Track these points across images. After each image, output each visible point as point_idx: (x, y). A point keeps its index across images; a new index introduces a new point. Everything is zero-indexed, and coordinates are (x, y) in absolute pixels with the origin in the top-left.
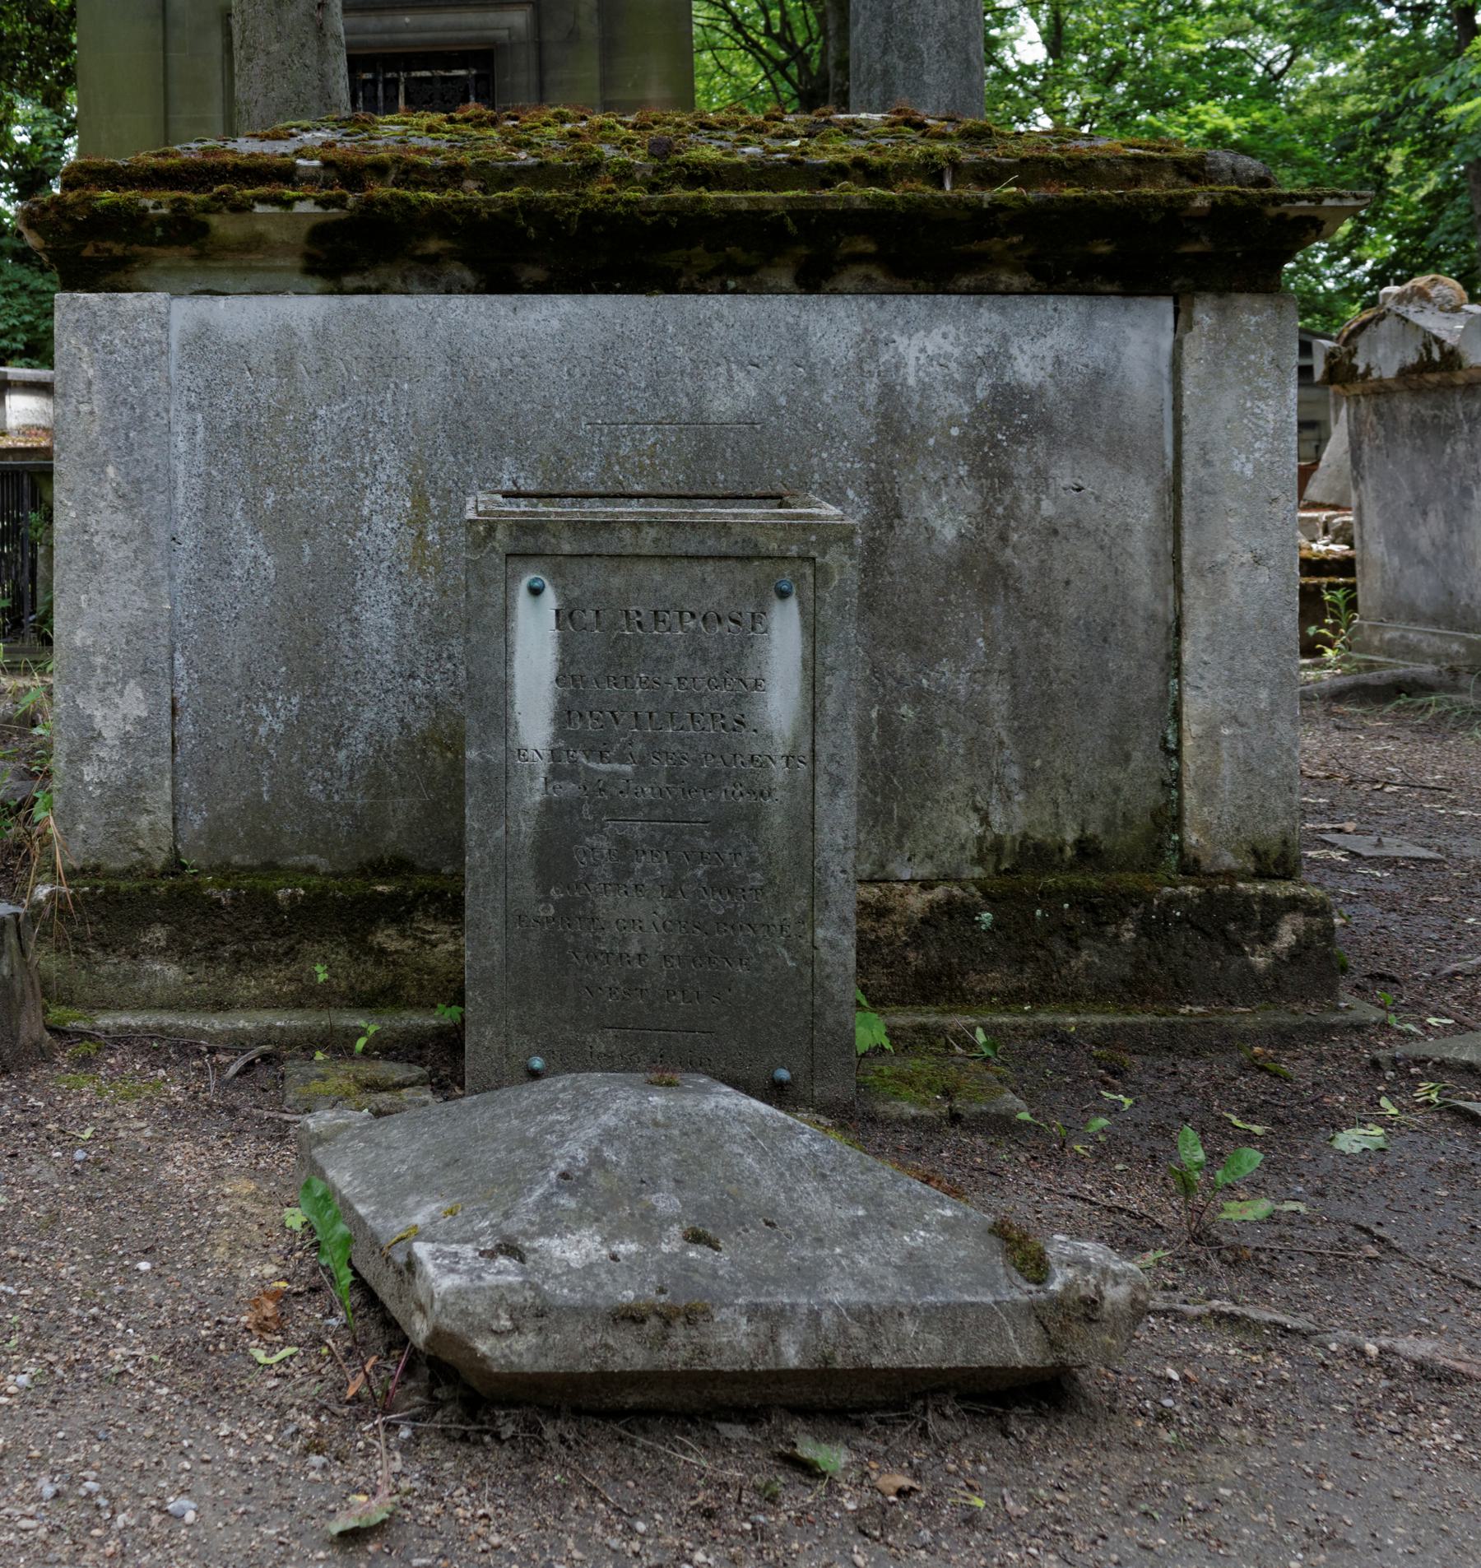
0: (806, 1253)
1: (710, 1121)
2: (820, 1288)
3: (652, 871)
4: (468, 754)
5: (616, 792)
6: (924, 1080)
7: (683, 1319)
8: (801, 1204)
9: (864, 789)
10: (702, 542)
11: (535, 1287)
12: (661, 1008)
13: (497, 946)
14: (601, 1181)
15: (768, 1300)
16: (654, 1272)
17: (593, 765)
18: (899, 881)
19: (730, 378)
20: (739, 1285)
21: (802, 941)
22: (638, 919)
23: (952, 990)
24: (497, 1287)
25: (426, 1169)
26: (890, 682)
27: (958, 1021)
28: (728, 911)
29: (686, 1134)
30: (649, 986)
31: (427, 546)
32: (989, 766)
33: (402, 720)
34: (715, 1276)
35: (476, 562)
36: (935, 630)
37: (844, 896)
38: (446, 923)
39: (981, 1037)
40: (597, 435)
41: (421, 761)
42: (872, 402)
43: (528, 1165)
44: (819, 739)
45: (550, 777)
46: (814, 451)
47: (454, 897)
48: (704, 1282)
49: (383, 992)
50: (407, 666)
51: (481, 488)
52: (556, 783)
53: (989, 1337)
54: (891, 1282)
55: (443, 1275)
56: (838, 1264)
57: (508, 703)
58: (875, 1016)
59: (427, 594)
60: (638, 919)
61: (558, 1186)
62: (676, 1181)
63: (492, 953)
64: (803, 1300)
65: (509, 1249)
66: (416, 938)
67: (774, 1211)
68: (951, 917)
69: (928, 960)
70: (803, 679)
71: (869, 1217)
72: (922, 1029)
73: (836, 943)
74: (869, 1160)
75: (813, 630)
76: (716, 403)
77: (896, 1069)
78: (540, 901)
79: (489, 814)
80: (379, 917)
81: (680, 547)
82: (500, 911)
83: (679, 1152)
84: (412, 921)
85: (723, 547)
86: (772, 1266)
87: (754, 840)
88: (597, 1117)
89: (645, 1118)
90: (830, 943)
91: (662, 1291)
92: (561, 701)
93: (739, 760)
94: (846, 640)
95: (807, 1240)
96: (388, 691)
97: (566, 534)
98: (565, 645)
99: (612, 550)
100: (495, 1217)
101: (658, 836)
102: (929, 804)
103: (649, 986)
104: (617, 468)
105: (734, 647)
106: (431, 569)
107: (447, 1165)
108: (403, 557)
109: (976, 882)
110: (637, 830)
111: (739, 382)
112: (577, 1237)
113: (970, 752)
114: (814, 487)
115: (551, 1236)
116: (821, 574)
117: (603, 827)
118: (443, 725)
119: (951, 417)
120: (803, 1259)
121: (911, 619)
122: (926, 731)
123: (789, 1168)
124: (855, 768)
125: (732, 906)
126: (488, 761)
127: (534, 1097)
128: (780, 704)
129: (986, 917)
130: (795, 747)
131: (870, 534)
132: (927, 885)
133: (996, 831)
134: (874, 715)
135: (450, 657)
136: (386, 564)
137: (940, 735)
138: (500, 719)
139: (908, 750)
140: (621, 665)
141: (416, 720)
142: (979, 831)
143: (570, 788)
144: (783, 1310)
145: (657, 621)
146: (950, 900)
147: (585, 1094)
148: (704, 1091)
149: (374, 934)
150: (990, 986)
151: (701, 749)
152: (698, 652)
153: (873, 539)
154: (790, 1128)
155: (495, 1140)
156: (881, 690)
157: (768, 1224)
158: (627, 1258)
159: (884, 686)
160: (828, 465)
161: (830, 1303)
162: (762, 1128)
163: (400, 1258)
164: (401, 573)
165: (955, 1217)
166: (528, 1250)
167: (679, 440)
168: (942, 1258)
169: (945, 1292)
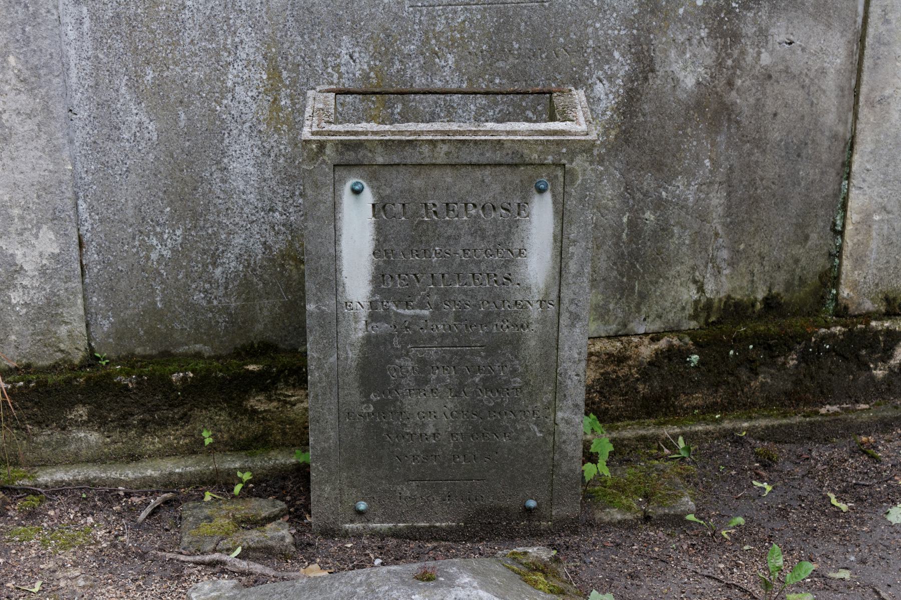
3: (444, 380)
4: (308, 307)
5: (418, 328)
10: (482, 154)
12: (449, 466)
13: (332, 434)
17: (400, 311)
21: (547, 420)
28: (497, 403)
30: (441, 453)
45: (369, 321)
52: (374, 324)
57: (337, 271)
60: (433, 412)
63: (329, 438)
70: (554, 248)
75: (562, 214)
78: (363, 403)
79: (324, 347)
82: (334, 411)
85: (498, 157)
87: (516, 357)
90: (566, 421)
93: (507, 304)
97: (380, 149)
99: (414, 161)
101: (448, 357)
103: (441, 453)
105: (504, 228)
110: (432, 353)
116: (570, 176)
125: (499, 400)
126: (323, 311)
128: (537, 265)
130: (547, 294)
145: (448, 210)
151: (479, 298)
152: (478, 232)
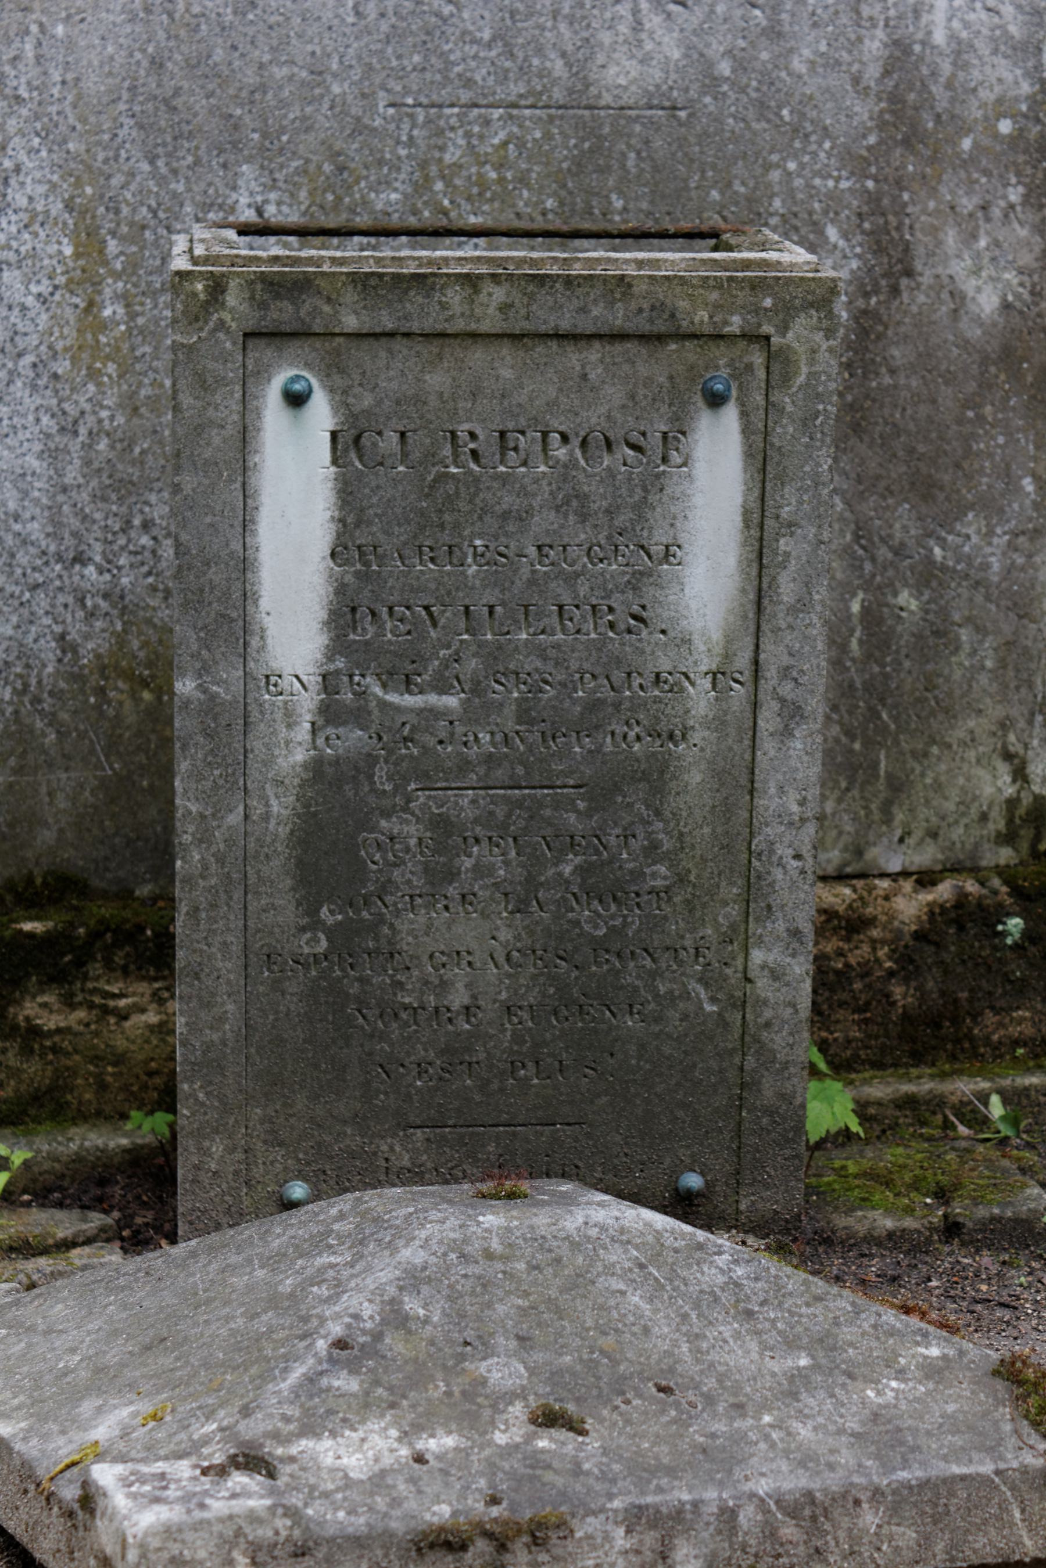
0: (720, 1427)
1: (576, 1246)
2: (738, 1473)
3: (491, 870)
4: (178, 686)
5: (431, 741)
6: (908, 1177)
7: (526, 1539)
8: (713, 1356)
9: (835, 730)
10: (583, 310)
11: (292, 1513)
12: (502, 1090)
13: (230, 1007)
14: (400, 1347)
15: (658, 1499)
16: (482, 1474)
17: (393, 698)
18: (883, 875)
19: (638, 26)
20: (614, 1481)
21: (729, 971)
22: (464, 950)
23: (957, 1041)
24: (231, 1517)
25: (112, 1357)
26: (884, 553)
27: (964, 1087)
28: (612, 930)
29: (537, 1267)
30: (482, 1056)
31: (103, 326)
32: (1031, 686)
33: (62, 637)
34: (577, 1471)
35: (190, 348)
36: (958, 466)
37: (798, 899)
38: (143, 978)
39: (996, 1108)
40: (406, 126)
41: (98, 707)
42: (873, 72)
43: (282, 1334)
44: (767, 644)
45: (320, 722)
46: (775, 158)
47: (156, 935)
48: (560, 1481)
49: (36, 1098)
50: (69, 541)
51: (198, 220)
52: (330, 731)
53: (985, 1522)
54: (846, 1458)
55: (142, 1508)
56: (767, 1437)
57: (248, 596)
58: (839, 1085)
59: (104, 414)
60: (464, 950)
61: (331, 1359)
62: (520, 1338)
63: (222, 1019)
64: (711, 1494)
65: (251, 1460)
66: (91, 1006)
67: (672, 1370)
68: (961, 928)
69: (923, 994)
70: (744, 544)
71: (816, 1367)
72: (909, 1102)
73: (782, 970)
74: (819, 1285)
75: (763, 462)
76: (613, 70)
77: (866, 1164)
78: (303, 929)
79: (216, 786)
80: (28, 975)
81: (547, 320)
82: (236, 949)
83: (526, 1294)
84: (86, 977)
85: (618, 318)
86: (665, 1449)
87: (658, 813)
88: (396, 1250)
89: (473, 1249)
90: (772, 971)
91: (494, 1501)
92: (341, 589)
93: (637, 681)
94: (816, 476)
95: (720, 1409)
96: (35, 587)
97: (350, 296)
98: (348, 494)
99: (428, 325)
100: (225, 1416)
101: (500, 813)
102: (935, 750)
103: (482, 1056)
104: (439, 186)
105: (631, 492)
106: (111, 368)
107: (148, 1348)
108: (60, 346)
109: (1000, 871)
110: (465, 804)
111: (651, 33)
112: (361, 1434)
113: (1003, 663)
114: (774, 221)
115: (318, 1436)
116: (780, 362)
117: (409, 801)
118: (135, 644)
119: (1000, 101)
120: (713, 1436)
121: (921, 448)
122: (937, 633)
123: (697, 1306)
124: (822, 689)
125: (618, 922)
126: (213, 697)
127: (290, 1232)
128: (704, 587)
129: (1015, 924)
130: (728, 656)
131: (860, 303)
132: (926, 879)
133: (1036, 789)
134: (855, 607)
135: (146, 526)
136: (29, 359)
137: (957, 638)
138: (232, 620)
139: (907, 664)
140: (442, 526)
141: (87, 637)
142: (1010, 791)
143: (353, 739)
144: (680, 1512)
145: (504, 449)
146: (962, 899)
147: (375, 1220)
148: (567, 1201)
149: (19, 1003)
150: (1014, 1031)
151: (574, 665)
152: (573, 502)
153: (865, 312)
154: (700, 1247)
155: (226, 1303)
156: (868, 567)
157: (661, 1389)
158: (439, 1457)
159: (873, 559)
160: (798, 182)
161: (753, 1495)
162: (656, 1250)
163: (70, 1493)
164: (55, 376)
165: (944, 1357)
166: (282, 1460)
167: (548, 136)
168: (921, 1418)
169: (923, 1464)
